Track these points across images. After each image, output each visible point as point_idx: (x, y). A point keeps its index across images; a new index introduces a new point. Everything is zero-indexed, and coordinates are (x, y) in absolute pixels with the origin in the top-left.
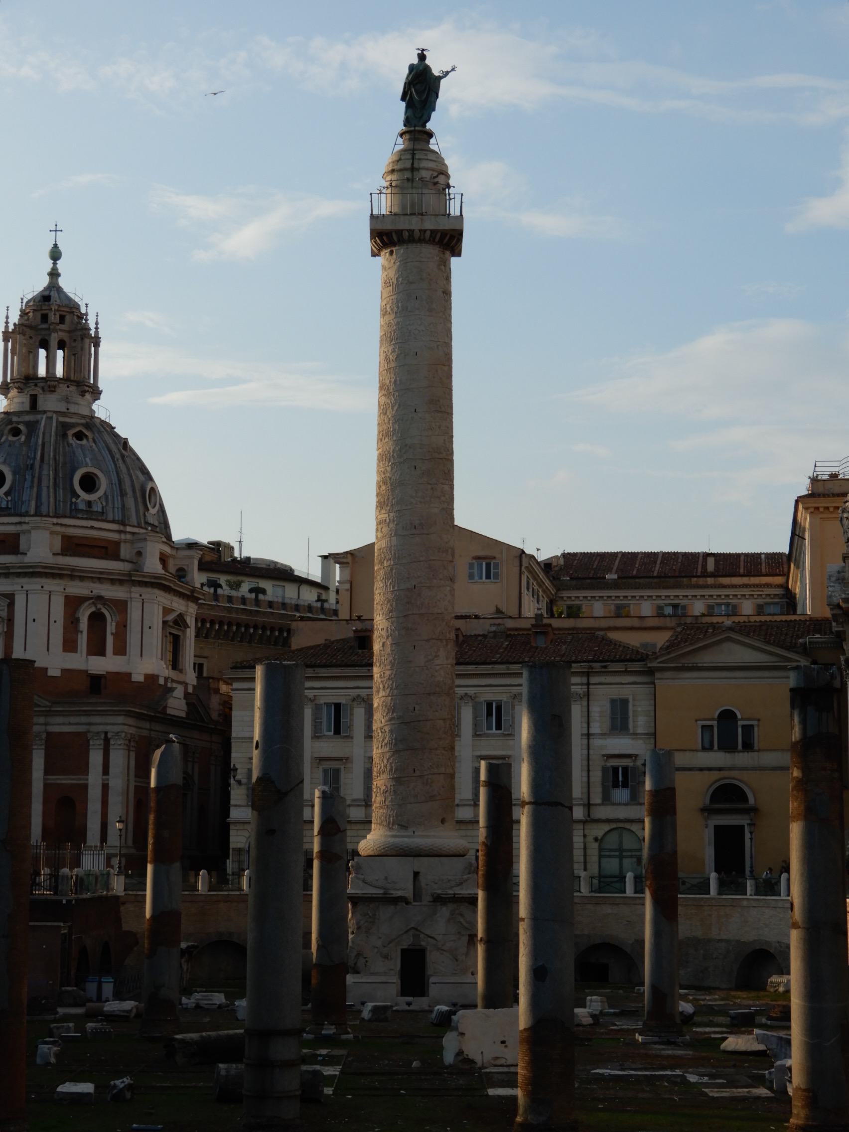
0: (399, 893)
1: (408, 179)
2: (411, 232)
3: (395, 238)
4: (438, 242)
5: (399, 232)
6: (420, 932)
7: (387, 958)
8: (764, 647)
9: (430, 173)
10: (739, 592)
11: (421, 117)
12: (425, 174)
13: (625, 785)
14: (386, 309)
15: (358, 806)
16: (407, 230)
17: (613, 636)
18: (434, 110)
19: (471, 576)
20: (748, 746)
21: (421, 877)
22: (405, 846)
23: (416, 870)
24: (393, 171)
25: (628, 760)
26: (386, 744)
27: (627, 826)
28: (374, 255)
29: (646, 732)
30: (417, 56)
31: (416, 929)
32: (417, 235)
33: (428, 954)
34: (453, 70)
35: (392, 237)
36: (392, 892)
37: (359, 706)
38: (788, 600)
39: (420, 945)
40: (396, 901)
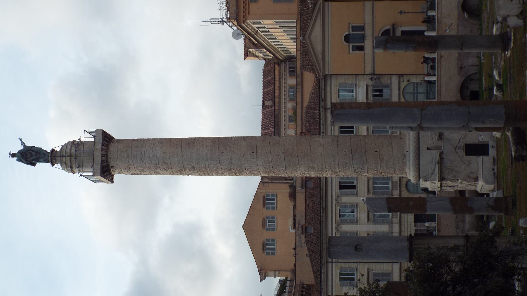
0: (438, 156)
1: (76, 158)
2: (102, 156)
3: (105, 164)
4: (108, 143)
5: (102, 162)
6: (457, 146)
7: (470, 162)
8: (313, 20)
9: (73, 147)
10: (283, 85)
11: (44, 154)
12: (73, 149)
13: (381, 91)
14: (141, 170)
15: (392, 228)
16: (101, 157)
17: (306, 103)
18: (41, 148)
19: (273, 208)
20: (362, 28)
21: (430, 147)
22: (414, 154)
23: (426, 149)
24: (71, 167)
25: (369, 88)
26: (363, 167)
27: (402, 90)
28: (112, 181)
29: (355, 80)
30: (13, 158)
31: (456, 148)
32: (104, 153)
33: (468, 142)
34: (21, 140)
35: (104, 166)
36: (437, 160)
37: (341, 227)
38: (287, 61)
39: (464, 146)
40: (441, 158)
